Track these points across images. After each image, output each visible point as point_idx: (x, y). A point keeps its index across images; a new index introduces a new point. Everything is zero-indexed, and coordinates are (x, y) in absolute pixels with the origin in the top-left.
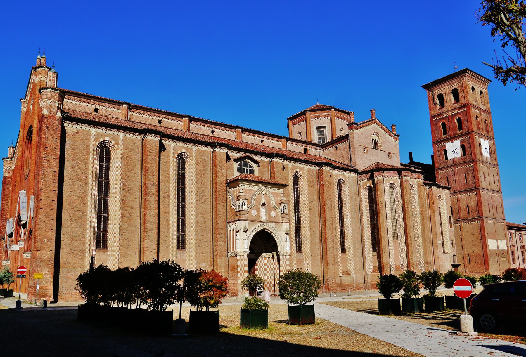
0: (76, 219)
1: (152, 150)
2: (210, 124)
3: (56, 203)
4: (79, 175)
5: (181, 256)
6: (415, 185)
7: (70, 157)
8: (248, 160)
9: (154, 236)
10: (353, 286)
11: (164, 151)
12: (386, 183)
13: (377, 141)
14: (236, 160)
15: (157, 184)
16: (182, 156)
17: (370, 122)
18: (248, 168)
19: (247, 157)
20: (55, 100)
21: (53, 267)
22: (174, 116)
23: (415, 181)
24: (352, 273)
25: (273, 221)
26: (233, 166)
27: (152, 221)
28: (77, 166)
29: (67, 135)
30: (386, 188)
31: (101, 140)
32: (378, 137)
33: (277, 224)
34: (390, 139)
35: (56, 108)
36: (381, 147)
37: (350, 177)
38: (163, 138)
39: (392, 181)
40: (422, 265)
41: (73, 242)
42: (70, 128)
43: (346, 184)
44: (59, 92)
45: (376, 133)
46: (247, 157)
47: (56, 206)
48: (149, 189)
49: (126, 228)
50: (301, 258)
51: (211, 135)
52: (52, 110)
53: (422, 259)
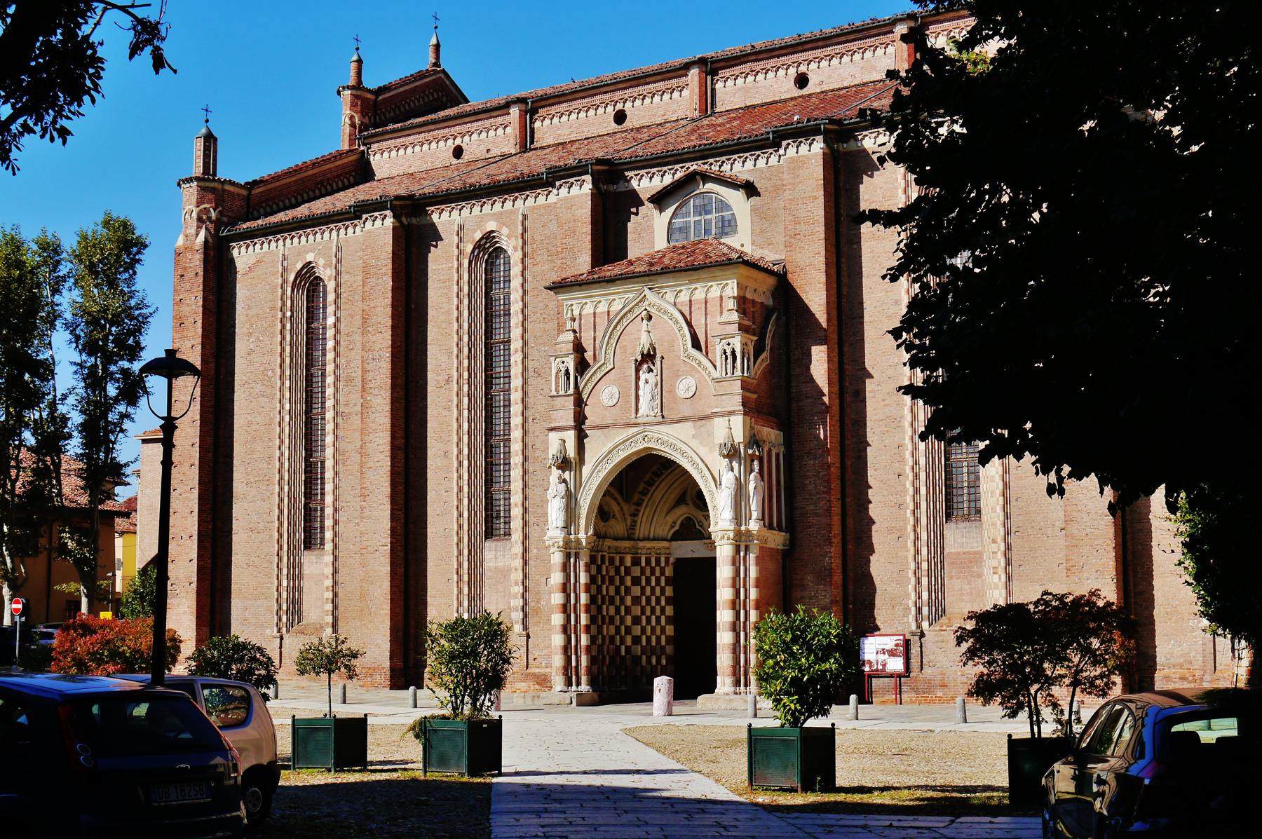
0: (257, 479)
1: (377, 258)
2: (786, 55)
3: (198, 449)
4: (261, 369)
5: (496, 558)
7: (245, 330)
8: (710, 186)
9: (382, 507)
11: (436, 246)
14: (660, 199)
15: (388, 355)
16: (497, 242)
18: (713, 216)
19: (698, 177)
20: (190, 207)
21: (194, 596)
22: (659, 77)
25: (688, 413)
26: (651, 228)
27: (378, 464)
28: (257, 348)
29: (239, 276)
31: (299, 266)
33: (699, 423)
35: (195, 224)
38: (432, 208)
41: (253, 536)
42: (242, 257)
44: (195, 183)
46: (698, 177)
47: (198, 455)
48: (371, 373)
49: (349, 489)
50: (975, 547)
51: (796, 92)
52: (188, 232)
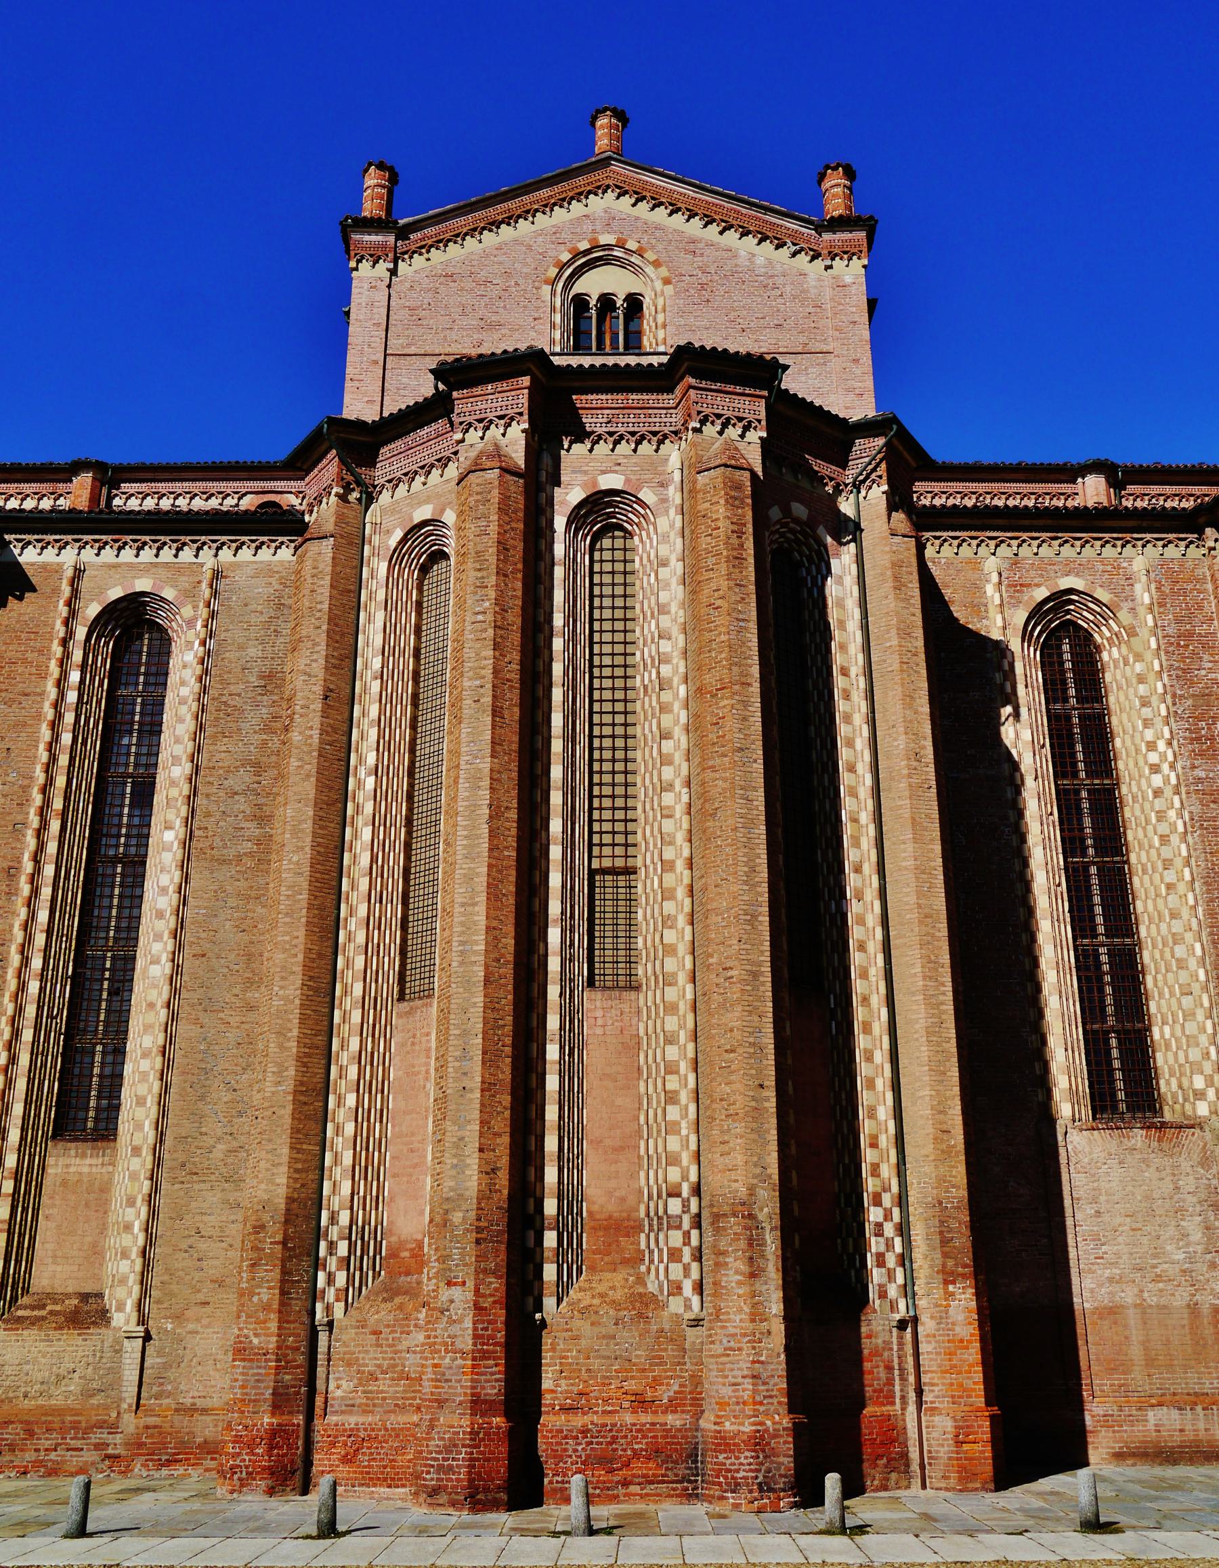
6: (671, 490)
10: (113, 1428)
12: (389, 532)
13: (634, 304)
17: (545, 193)
23: (673, 454)
24: (121, 1307)
30: (377, 569)
32: (637, 270)
34: (770, 262)
36: (661, 334)
37: (240, 578)
39: (427, 501)
40: (676, 1238)
43: (191, 623)
45: (608, 247)
53: (682, 1174)
